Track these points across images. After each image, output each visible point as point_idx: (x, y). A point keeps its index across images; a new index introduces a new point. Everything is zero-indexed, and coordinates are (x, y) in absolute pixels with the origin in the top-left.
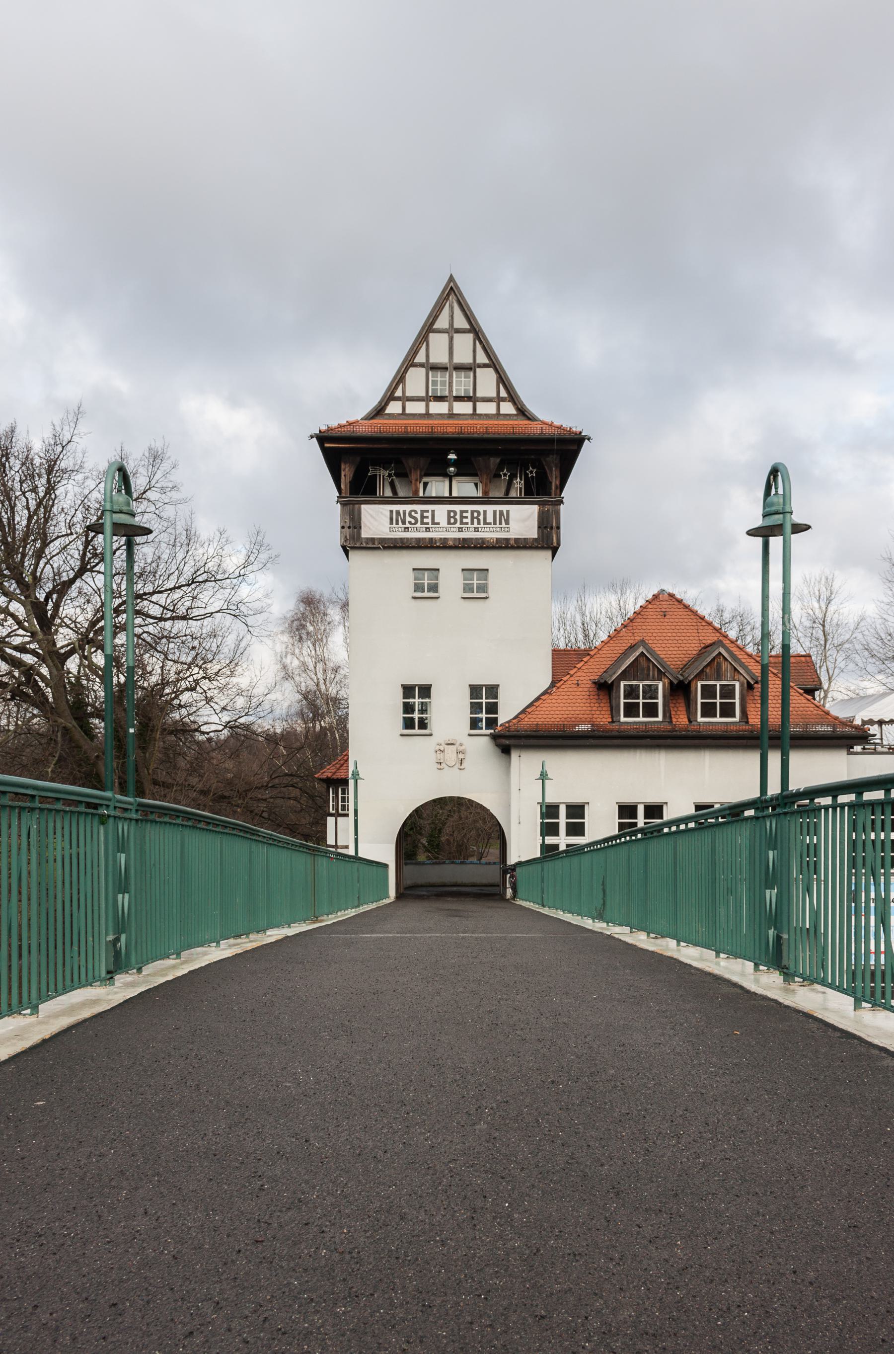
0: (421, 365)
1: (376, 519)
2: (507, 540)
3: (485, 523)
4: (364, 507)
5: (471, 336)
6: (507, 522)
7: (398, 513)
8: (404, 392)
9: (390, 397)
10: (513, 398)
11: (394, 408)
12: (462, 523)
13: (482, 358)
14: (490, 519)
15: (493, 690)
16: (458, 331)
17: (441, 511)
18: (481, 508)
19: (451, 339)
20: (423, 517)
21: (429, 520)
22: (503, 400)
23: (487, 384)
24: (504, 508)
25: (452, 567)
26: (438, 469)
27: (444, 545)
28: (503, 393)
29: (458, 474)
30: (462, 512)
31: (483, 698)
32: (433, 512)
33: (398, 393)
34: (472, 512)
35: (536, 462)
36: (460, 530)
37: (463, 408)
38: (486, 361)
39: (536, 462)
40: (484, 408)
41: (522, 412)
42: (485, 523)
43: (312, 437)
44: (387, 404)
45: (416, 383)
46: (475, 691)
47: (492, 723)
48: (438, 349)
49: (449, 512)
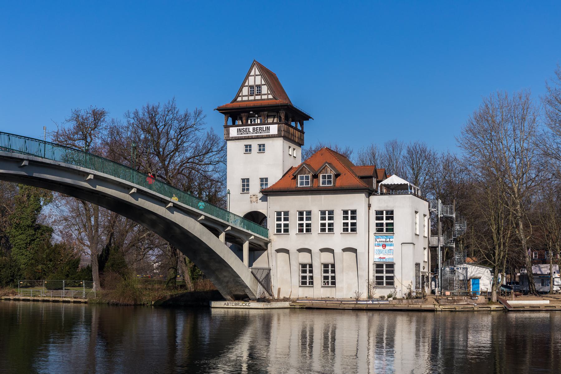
4: (231, 128)
11: (239, 99)
13: (263, 83)
15: (266, 179)
16: (257, 75)
23: (265, 89)
24: (268, 126)
25: (255, 144)
31: (264, 181)
33: (241, 95)
37: (258, 97)
40: (264, 97)
45: (245, 91)
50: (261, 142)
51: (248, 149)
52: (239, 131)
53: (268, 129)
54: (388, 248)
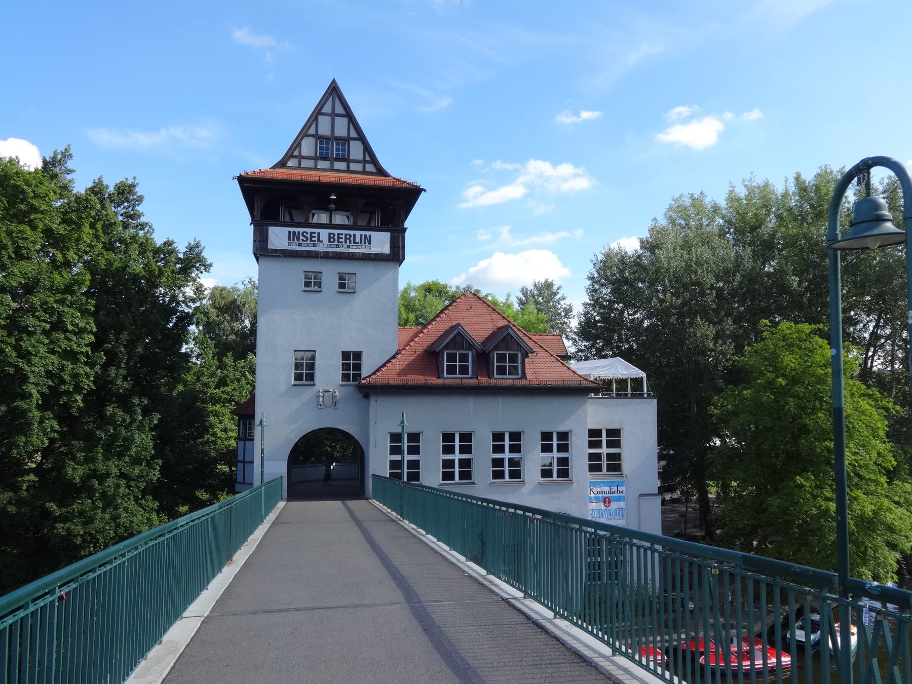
0: (312, 136)
1: (279, 237)
2: (370, 254)
3: (355, 242)
4: (270, 228)
5: (345, 120)
6: (369, 243)
7: (294, 233)
8: (300, 152)
9: (289, 155)
10: (374, 161)
11: (292, 163)
12: (338, 242)
13: (353, 134)
14: (358, 240)
15: (358, 355)
16: (338, 115)
17: (324, 234)
18: (352, 232)
19: (333, 121)
20: (311, 237)
21: (316, 239)
22: (368, 162)
23: (356, 151)
24: (368, 233)
26: (324, 206)
27: (326, 256)
28: (368, 158)
29: (335, 210)
30: (339, 234)
31: (352, 361)
32: (319, 234)
33: (296, 153)
34: (346, 235)
35: (388, 205)
36: (337, 246)
38: (356, 136)
39: (388, 205)
41: (381, 172)
42: (355, 242)
43: (234, 178)
44: (288, 160)
46: (346, 355)
47: (357, 377)
49: (330, 234)
50: (346, 267)
51: (313, 283)
52: (292, 236)
53: (368, 240)
54: (614, 505)
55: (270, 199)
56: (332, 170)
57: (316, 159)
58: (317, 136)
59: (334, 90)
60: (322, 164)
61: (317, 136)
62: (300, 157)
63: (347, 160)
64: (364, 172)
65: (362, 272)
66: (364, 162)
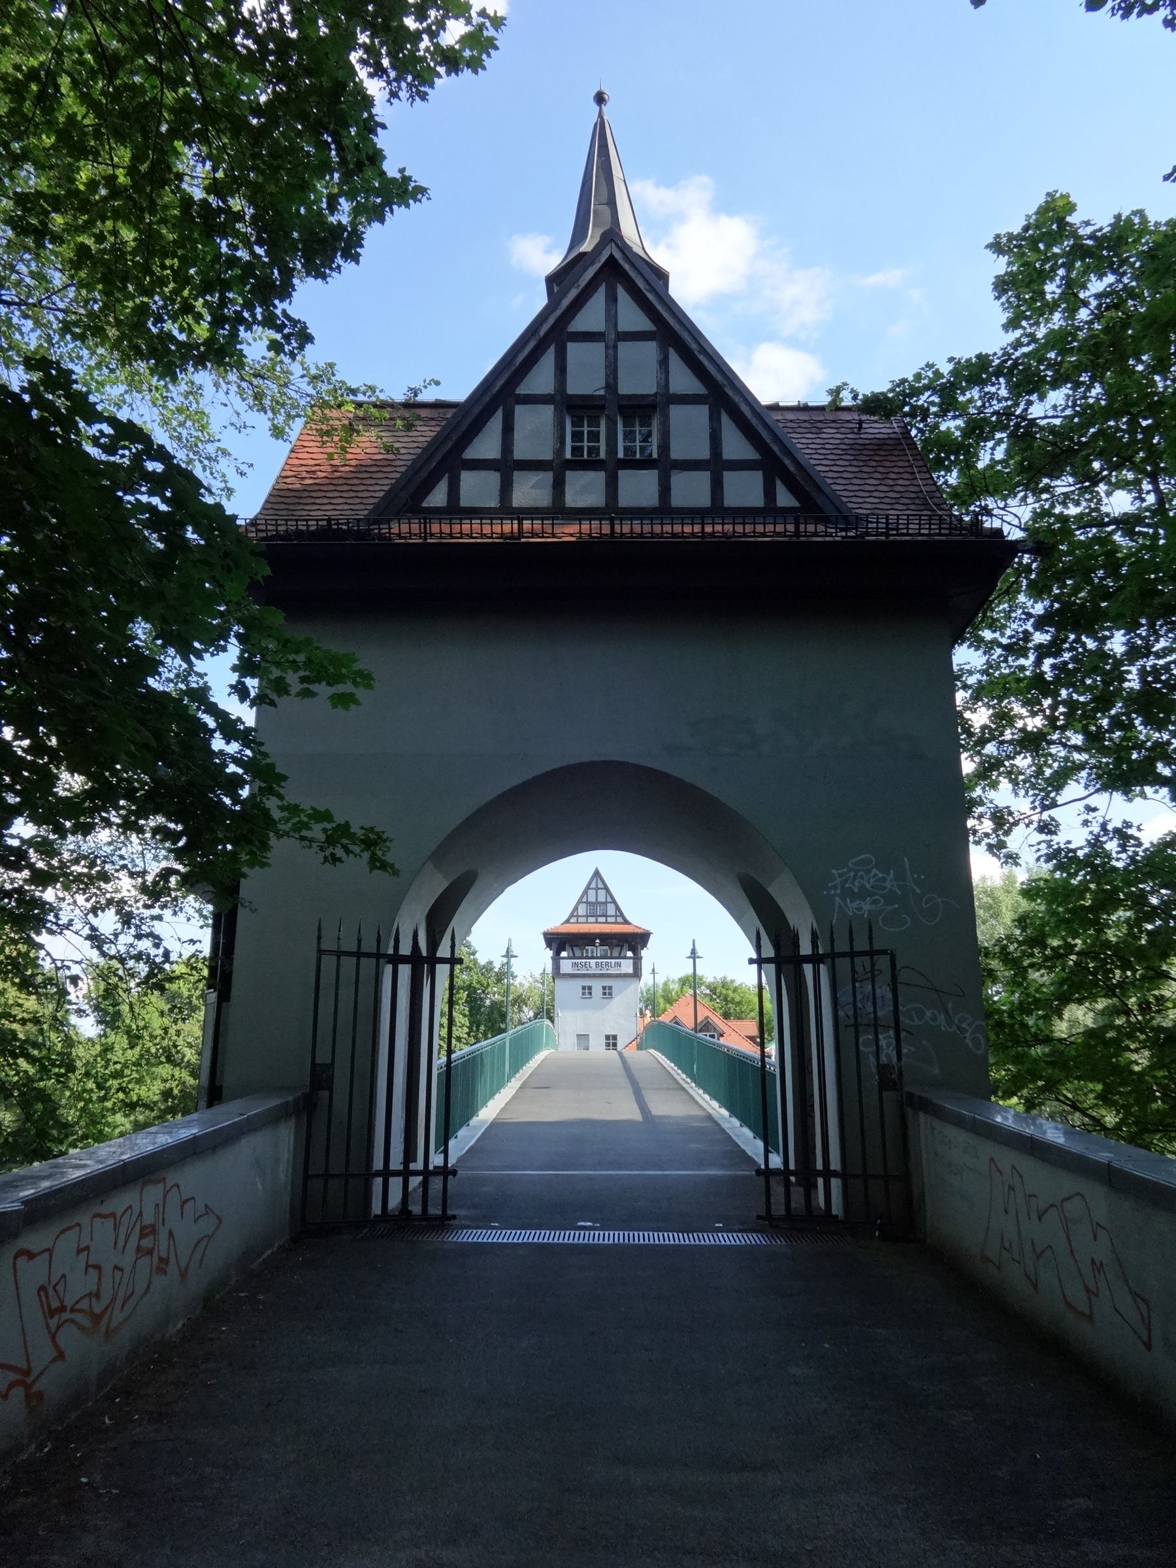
9: (572, 915)
13: (609, 899)
15: (615, 1037)
23: (611, 910)
25: (597, 986)
27: (594, 976)
35: (635, 941)
39: (635, 941)
41: (626, 922)
46: (608, 1037)
48: (592, 898)
53: (619, 965)
55: (558, 942)
56: (597, 922)
57: (587, 916)
58: (587, 902)
59: (597, 874)
60: (591, 919)
61: (587, 902)
62: (578, 916)
63: (606, 916)
64: (616, 923)
65: (615, 984)
66: (616, 916)
